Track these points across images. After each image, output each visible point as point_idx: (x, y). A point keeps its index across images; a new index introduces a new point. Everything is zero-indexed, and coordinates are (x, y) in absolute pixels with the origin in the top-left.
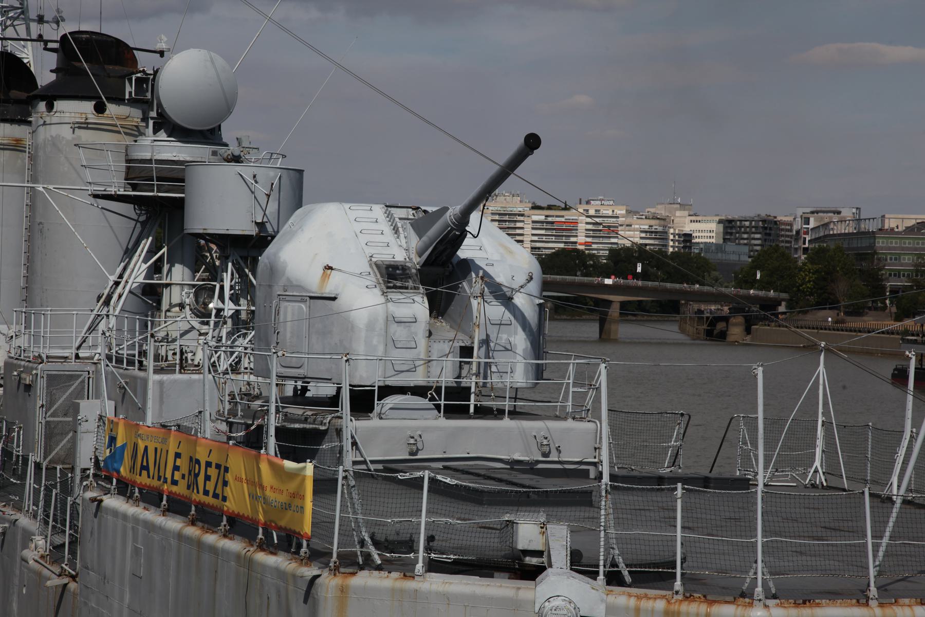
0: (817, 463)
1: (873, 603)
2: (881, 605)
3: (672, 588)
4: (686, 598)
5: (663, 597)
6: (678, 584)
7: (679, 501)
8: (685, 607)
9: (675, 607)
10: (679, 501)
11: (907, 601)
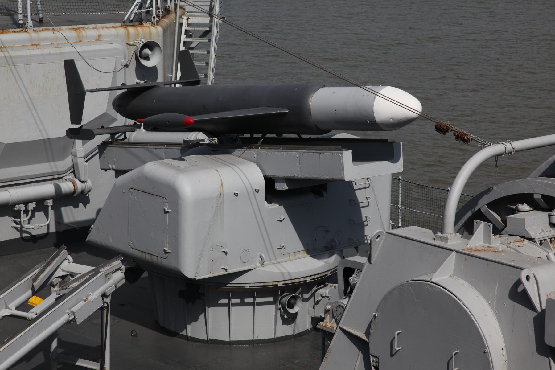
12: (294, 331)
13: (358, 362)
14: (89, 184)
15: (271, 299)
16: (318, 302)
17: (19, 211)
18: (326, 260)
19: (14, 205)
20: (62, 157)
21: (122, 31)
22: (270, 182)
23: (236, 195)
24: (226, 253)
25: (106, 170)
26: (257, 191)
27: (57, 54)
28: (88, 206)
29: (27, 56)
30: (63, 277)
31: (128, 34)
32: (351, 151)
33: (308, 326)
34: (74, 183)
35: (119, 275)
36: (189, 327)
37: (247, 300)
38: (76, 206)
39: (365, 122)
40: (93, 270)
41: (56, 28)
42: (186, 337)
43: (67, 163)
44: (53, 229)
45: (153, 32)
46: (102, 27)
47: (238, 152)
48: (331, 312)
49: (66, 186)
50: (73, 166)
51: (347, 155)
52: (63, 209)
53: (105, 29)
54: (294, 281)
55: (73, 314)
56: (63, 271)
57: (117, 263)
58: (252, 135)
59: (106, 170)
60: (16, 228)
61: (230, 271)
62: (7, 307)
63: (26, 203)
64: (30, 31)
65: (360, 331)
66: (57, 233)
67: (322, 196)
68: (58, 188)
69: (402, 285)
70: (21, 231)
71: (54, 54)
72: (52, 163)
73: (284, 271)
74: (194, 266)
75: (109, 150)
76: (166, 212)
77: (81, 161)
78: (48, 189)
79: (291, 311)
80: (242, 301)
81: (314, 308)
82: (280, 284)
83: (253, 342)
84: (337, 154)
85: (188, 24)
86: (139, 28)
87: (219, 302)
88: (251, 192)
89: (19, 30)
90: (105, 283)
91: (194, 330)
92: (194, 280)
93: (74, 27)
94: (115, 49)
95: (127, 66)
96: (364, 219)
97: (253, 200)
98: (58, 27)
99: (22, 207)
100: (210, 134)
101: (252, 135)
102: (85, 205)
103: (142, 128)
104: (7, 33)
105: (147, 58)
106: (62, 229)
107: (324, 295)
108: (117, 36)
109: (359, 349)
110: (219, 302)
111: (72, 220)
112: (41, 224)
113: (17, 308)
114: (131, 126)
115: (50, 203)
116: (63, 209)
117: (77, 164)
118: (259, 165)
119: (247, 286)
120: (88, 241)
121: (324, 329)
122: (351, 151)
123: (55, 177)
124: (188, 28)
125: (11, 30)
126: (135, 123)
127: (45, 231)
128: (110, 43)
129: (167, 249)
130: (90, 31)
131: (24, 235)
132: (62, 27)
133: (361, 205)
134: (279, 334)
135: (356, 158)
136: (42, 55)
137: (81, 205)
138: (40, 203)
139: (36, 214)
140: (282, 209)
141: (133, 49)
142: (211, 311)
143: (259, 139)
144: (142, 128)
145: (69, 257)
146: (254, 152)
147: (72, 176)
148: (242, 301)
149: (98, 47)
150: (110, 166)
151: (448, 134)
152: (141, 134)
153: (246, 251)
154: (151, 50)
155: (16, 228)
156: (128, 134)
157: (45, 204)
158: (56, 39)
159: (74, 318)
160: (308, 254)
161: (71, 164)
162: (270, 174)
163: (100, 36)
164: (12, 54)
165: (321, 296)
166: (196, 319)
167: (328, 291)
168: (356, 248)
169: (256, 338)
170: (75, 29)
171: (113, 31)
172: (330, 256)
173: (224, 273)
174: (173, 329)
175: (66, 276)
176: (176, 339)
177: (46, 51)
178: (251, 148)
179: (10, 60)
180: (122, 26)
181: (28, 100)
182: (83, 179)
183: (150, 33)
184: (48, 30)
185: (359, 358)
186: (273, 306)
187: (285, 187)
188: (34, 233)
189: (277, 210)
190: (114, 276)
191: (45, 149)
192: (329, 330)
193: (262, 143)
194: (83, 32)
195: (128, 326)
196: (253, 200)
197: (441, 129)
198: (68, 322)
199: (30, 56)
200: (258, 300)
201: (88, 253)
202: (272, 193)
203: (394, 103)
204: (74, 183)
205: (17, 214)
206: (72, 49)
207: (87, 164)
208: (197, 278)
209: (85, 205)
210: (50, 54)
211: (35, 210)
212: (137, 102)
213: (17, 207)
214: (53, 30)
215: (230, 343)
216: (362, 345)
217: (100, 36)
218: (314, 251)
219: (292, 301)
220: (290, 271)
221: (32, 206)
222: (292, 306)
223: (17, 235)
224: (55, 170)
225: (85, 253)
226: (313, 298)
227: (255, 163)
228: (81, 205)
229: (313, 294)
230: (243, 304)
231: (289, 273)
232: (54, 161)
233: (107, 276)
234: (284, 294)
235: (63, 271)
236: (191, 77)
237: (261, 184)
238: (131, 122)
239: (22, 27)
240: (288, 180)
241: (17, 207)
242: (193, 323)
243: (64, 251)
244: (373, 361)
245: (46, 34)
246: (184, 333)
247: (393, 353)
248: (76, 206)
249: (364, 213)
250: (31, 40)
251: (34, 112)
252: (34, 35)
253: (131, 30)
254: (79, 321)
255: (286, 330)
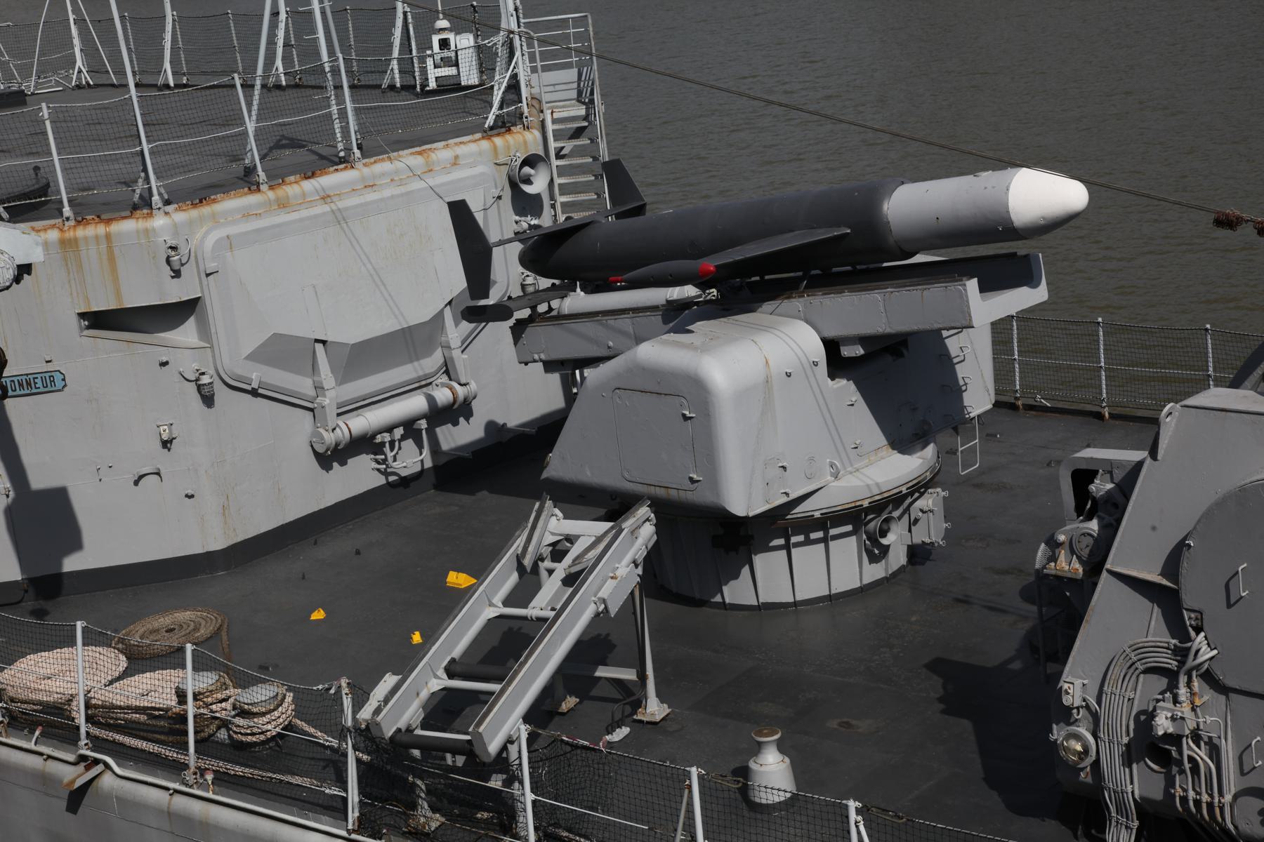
0: (79, 63)
1: (264, 187)
2: (271, 188)
3: (61, 214)
4: (79, 223)
5: (53, 226)
6: (67, 211)
7: (48, 123)
8: (81, 232)
9: (70, 234)
10: (48, 123)
11: (292, 178)
12: (886, 570)
13: (1153, 623)
14: (473, 386)
15: (849, 528)
16: (916, 521)
17: (383, 444)
18: (919, 454)
19: (374, 436)
20: (429, 352)
21: (485, 144)
22: (831, 346)
23: (788, 375)
24: (784, 468)
25: (526, 364)
26: (815, 364)
27: (402, 195)
28: (471, 419)
29: (361, 205)
30: (554, 544)
31: (495, 148)
32: (976, 280)
33: (903, 560)
34: (451, 388)
35: (648, 531)
36: (725, 589)
37: (814, 536)
38: (456, 423)
39: (998, 229)
40: (612, 528)
41: (393, 155)
42: (723, 605)
43: (433, 362)
44: (428, 464)
45: (524, 141)
46: (456, 144)
47: (768, 306)
48: (1067, 544)
49: (443, 396)
50: (446, 364)
51: (972, 285)
52: (438, 430)
53: (462, 146)
54: (886, 495)
55: (604, 601)
56: (553, 534)
57: (644, 511)
58: (762, 278)
59: (526, 364)
60: (378, 470)
61: (793, 496)
62: (491, 605)
63: (390, 429)
64: (359, 165)
65: (1150, 572)
66: (435, 468)
67: (902, 355)
68: (431, 399)
69: (1242, 489)
70: (385, 473)
71: (398, 196)
72: (416, 364)
73: (870, 482)
74: (744, 499)
75: (530, 331)
76: (685, 418)
77: (456, 354)
78: (415, 404)
79: (884, 541)
80: (807, 537)
81: (910, 531)
82: (866, 504)
83: (830, 598)
84: (954, 287)
85: (554, 121)
86: (508, 137)
87: (772, 544)
88: (807, 366)
89: (342, 166)
90: (632, 544)
91: (737, 592)
92: (747, 518)
93: (418, 149)
94: (482, 174)
95: (499, 198)
96: (961, 383)
97: (812, 380)
98: (395, 154)
99: (386, 437)
100: (703, 285)
101: (762, 278)
102: (467, 420)
103: (578, 290)
104: (326, 173)
105: (528, 181)
106: (443, 460)
107: (926, 509)
108: (480, 153)
109: (1152, 601)
110: (772, 544)
111: (453, 445)
112: (410, 459)
113: (507, 602)
114: (547, 290)
115: (423, 424)
116: (438, 430)
117: (452, 359)
118: (807, 322)
119: (817, 514)
120: (547, 479)
121: (1059, 573)
122: (976, 280)
123: (421, 384)
124: (557, 127)
125: (332, 169)
126: (553, 284)
127: (418, 468)
128: (472, 165)
129: (695, 477)
130: (442, 152)
131: (392, 478)
132: (401, 153)
133: (955, 361)
134: (867, 580)
135: (984, 288)
136: (382, 200)
137: (462, 420)
138: (409, 427)
139: (403, 444)
140: (851, 386)
141: (505, 169)
142: (759, 560)
143: (800, 279)
144: (578, 290)
145: (557, 511)
146: (797, 304)
147: (445, 379)
148: (807, 537)
149: (457, 174)
150: (536, 357)
151: (1239, 230)
152: (578, 300)
153: (812, 459)
154: (532, 167)
155: (378, 470)
156: (555, 304)
157: (415, 426)
158: (397, 172)
159: (606, 608)
160: (893, 449)
161: (442, 360)
162: (831, 333)
163: (457, 157)
164: (341, 204)
165: (922, 511)
166: (736, 576)
167: (930, 502)
168: (956, 429)
169: (833, 592)
170: (420, 153)
171: (473, 147)
172: (924, 447)
173: (784, 500)
174: (697, 596)
175: (558, 541)
176: (705, 609)
177: (387, 193)
178: (789, 298)
179: (338, 214)
180: (483, 138)
181: (372, 272)
182: (463, 381)
183: (525, 142)
184: (383, 160)
185: (1154, 615)
186: (854, 538)
187: (859, 351)
188: (404, 473)
189: (845, 388)
190: (641, 531)
191: (411, 340)
192: (1069, 575)
193: (806, 287)
194: (433, 156)
195: (652, 601)
196: (812, 380)
197: (1226, 222)
198: (597, 615)
199: (366, 204)
200: (833, 532)
201: (491, 492)
202: (837, 364)
203: (1041, 193)
204: (451, 388)
205: (377, 449)
206: (421, 185)
207: (465, 356)
208: (751, 514)
209: (467, 420)
210: (392, 197)
211: (403, 438)
212: (567, 250)
213: (379, 439)
214: (390, 158)
215: (795, 604)
216: (1165, 597)
217: (457, 157)
218: (902, 442)
219: (885, 527)
220: (880, 480)
221: (399, 432)
222: (884, 533)
223: (380, 480)
224: (421, 373)
225: (485, 493)
226: (906, 516)
227: (800, 319)
228: (462, 420)
229: (908, 509)
230: (808, 542)
231: (877, 484)
232: (418, 359)
233: (634, 532)
234: (869, 517)
235: (553, 534)
236: (627, 199)
237: (817, 351)
238: (545, 283)
239: (345, 161)
240: (863, 340)
241: (379, 439)
242: (732, 583)
243: (549, 503)
244: (1190, 618)
245: (382, 167)
246: (718, 599)
247: (1233, 600)
248: (456, 423)
249: (961, 371)
250: (363, 179)
251: (382, 288)
252: (366, 171)
253: (498, 141)
254: (613, 611)
255: (875, 572)
